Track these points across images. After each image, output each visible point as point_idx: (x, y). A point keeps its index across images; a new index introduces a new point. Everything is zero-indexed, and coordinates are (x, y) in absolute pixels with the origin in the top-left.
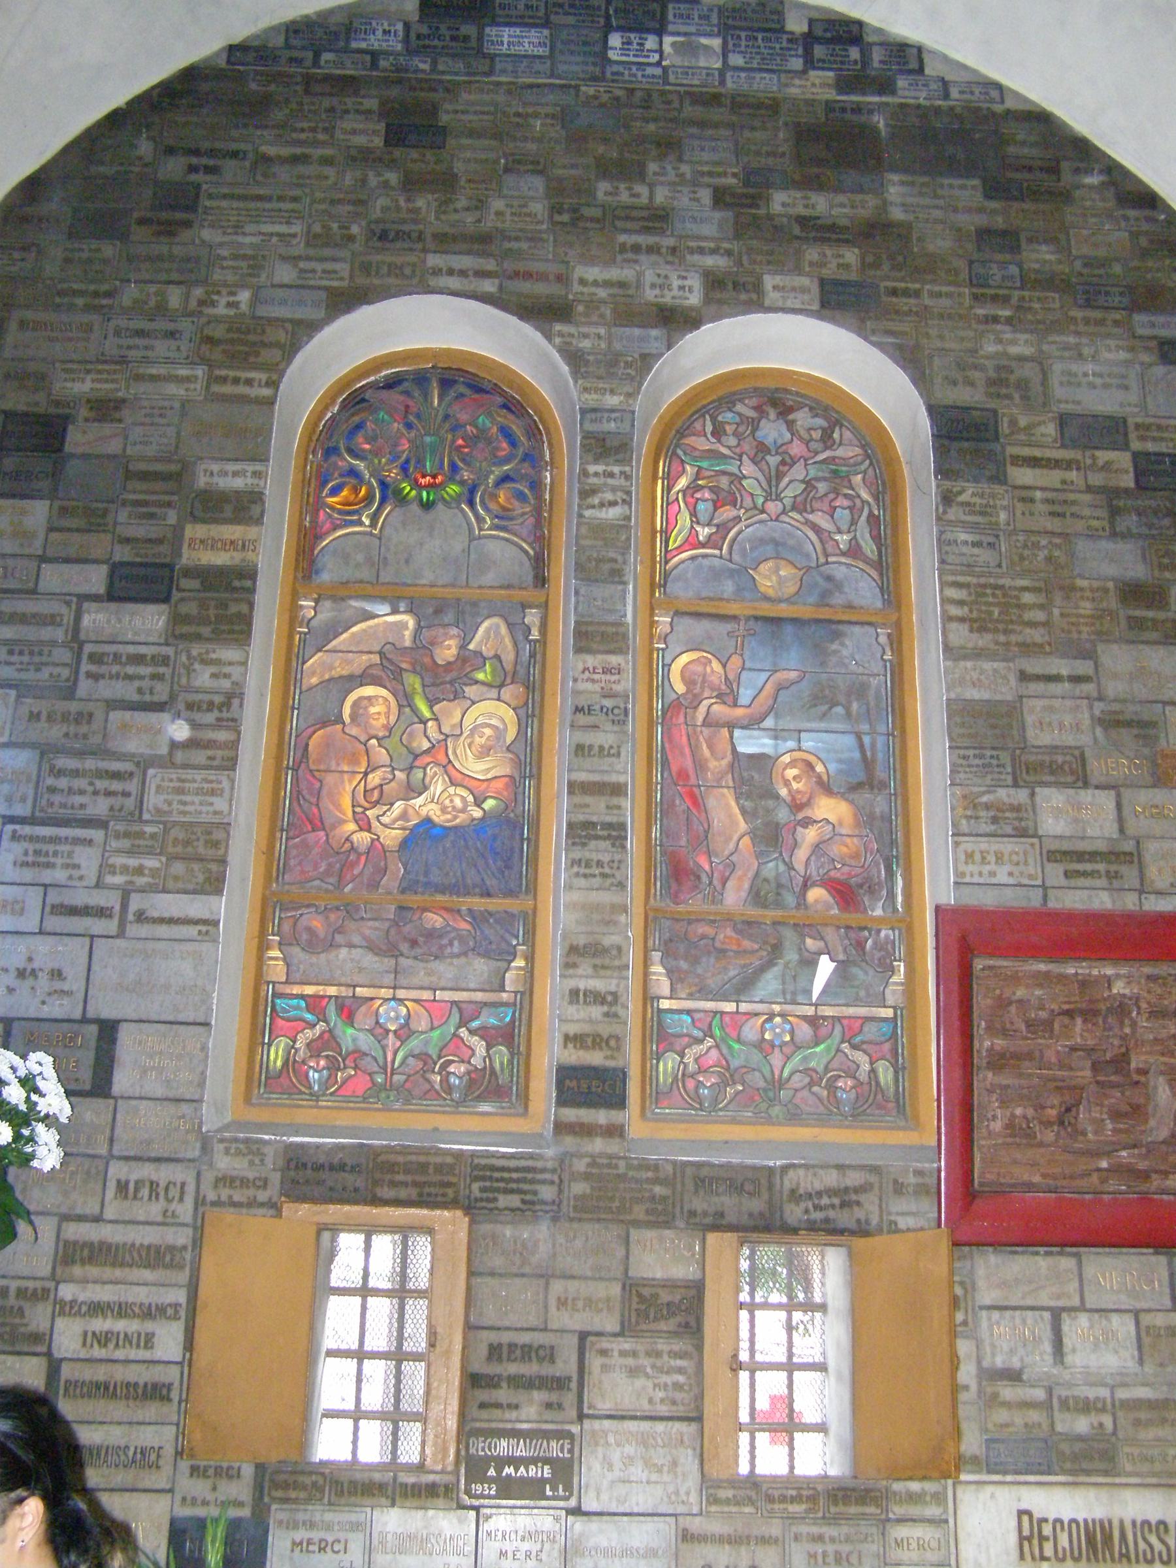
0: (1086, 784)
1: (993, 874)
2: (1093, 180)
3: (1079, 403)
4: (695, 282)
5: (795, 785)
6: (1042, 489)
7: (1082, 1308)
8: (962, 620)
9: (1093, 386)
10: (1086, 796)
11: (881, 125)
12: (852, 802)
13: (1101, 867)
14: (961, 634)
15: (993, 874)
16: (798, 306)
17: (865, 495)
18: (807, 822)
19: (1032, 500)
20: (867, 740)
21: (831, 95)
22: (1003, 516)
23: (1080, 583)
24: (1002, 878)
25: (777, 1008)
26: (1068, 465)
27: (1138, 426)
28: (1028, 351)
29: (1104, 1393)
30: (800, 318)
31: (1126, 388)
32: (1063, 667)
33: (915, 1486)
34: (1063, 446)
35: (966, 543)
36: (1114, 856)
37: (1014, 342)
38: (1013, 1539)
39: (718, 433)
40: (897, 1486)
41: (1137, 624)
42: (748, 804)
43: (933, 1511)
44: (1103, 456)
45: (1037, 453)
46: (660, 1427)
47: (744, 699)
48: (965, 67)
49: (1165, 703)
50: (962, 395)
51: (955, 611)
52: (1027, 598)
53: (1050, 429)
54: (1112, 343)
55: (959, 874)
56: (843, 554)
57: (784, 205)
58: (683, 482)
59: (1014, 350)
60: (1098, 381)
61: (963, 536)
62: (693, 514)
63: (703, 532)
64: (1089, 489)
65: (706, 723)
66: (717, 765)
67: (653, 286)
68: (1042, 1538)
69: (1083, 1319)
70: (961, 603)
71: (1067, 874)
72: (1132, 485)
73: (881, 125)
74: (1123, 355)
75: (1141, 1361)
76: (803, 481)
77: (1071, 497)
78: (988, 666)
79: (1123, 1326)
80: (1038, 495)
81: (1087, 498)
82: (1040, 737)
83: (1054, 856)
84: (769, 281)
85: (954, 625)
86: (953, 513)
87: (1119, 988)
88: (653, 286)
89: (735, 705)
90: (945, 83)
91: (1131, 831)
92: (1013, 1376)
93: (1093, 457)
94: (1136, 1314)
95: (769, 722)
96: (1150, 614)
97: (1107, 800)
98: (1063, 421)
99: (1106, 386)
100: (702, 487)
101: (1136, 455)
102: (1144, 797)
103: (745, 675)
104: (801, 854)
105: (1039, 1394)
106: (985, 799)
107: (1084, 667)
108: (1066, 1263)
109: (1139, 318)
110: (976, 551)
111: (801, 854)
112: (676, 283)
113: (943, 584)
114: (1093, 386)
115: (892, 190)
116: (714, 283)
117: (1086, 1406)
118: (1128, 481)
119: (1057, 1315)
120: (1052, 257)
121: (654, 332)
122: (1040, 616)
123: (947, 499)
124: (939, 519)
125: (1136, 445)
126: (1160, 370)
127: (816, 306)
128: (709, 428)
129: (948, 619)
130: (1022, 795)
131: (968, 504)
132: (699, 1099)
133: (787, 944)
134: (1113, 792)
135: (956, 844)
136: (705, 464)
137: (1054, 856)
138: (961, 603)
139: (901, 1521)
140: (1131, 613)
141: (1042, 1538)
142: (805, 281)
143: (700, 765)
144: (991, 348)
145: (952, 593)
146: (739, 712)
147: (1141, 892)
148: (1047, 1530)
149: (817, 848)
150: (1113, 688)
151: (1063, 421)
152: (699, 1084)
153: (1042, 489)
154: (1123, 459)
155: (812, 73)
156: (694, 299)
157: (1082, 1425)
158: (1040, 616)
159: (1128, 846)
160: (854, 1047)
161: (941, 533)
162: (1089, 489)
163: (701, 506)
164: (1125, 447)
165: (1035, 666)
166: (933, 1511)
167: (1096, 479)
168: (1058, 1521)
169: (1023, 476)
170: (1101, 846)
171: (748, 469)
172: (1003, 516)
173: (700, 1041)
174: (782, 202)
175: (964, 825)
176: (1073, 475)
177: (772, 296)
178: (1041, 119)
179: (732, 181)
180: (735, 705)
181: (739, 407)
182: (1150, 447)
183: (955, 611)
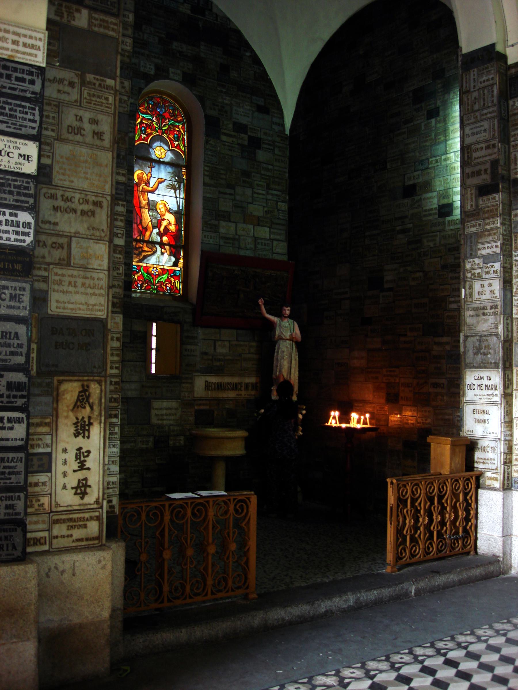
0: (230, 221)
1: (209, 241)
2: (248, 54)
3: (238, 119)
4: (153, 67)
5: (162, 210)
6: (228, 142)
7: (220, 340)
8: (207, 176)
9: (241, 115)
10: (230, 224)
11: (201, 26)
12: (174, 216)
13: (231, 241)
14: (207, 180)
15: (209, 241)
16: (177, 79)
17: (182, 132)
18: (164, 220)
19: (224, 145)
20: (178, 199)
21: (189, 12)
22: (219, 149)
23: (234, 169)
24: (211, 242)
25: (155, 266)
26: (234, 136)
27: (250, 128)
28: (228, 102)
29: (222, 357)
30: (177, 83)
31: (248, 117)
32: (228, 191)
33: (187, 376)
34: (233, 131)
35: (210, 155)
36: (234, 239)
37: (225, 99)
38: (204, 386)
39: (148, 106)
40: (183, 376)
41: (244, 182)
42: (151, 214)
43: (190, 381)
44: (242, 135)
45: (227, 132)
46: (138, 363)
47: (151, 185)
48: (222, 11)
49: (248, 203)
50: (214, 113)
51: (206, 173)
52: (222, 172)
53: (231, 126)
54: (247, 103)
55: (203, 240)
56: (176, 147)
57: (176, 46)
58: (139, 120)
59: (226, 102)
60: (243, 114)
61: (209, 153)
62: (141, 130)
63: (144, 136)
64: (238, 144)
65: (142, 191)
66: (144, 203)
67: (143, 66)
68: (210, 386)
69: (220, 343)
70: (208, 171)
71: (225, 243)
72: (247, 144)
73: (201, 26)
74: (249, 108)
75: (230, 351)
76: (168, 125)
77: (234, 145)
78: (212, 188)
79: (227, 344)
80: (227, 144)
81: (237, 146)
82: (222, 208)
83: (222, 238)
84: (171, 70)
85: (206, 177)
86: (208, 146)
87: (236, 272)
88: (143, 66)
89: (149, 187)
90: (217, 16)
91: (238, 233)
92: (206, 354)
93: (240, 135)
94: (230, 341)
95: (156, 192)
96: (247, 180)
97: (233, 225)
98: (235, 124)
99: (244, 116)
100: (143, 123)
101: (250, 137)
102: (241, 226)
103: (151, 178)
104: (162, 228)
105: (211, 357)
106: (209, 222)
107: (232, 191)
108: (217, 330)
109: (254, 98)
110: (212, 157)
111: (162, 228)
112: (148, 66)
113: (205, 166)
114: (241, 115)
115: (202, 47)
116: (158, 68)
117: (219, 360)
118: (246, 143)
119: (215, 341)
120: (236, 75)
121: (142, 81)
122: (224, 177)
123: (207, 142)
124: (205, 147)
125: (249, 133)
126: (256, 114)
127: (181, 80)
128: (146, 105)
129: (205, 175)
130: (216, 222)
131: (211, 144)
132: (138, 287)
133: (158, 250)
134: (235, 224)
135: (202, 233)
136: (144, 116)
137: (222, 238)
138: (208, 171)
139: (184, 383)
140: (245, 179)
141: (210, 386)
142: (179, 72)
143: (140, 202)
144: (220, 100)
145: (206, 168)
146: (150, 189)
147: (239, 248)
148: (210, 385)
149: (166, 227)
150: (238, 198)
151: (235, 124)
152: (138, 283)
153: (228, 142)
154: (245, 137)
155: (186, 5)
156: (152, 72)
157: (218, 364)
158: (224, 177)
159: (237, 237)
160: (171, 277)
161: (205, 151)
162: (238, 144)
163: (143, 129)
164: (246, 133)
165: (222, 190)
166: (190, 381)
167: (240, 142)
168: (213, 383)
169: (224, 138)
170: (231, 236)
171: (154, 119)
172: (219, 149)
173: (138, 273)
174: (175, 45)
175: (204, 228)
176: (235, 140)
177: (171, 75)
178: (238, 32)
179: (163, 36)
180: (149, 187)
181: (154, 100)
182: (252, 135)
183: (206, 173)
